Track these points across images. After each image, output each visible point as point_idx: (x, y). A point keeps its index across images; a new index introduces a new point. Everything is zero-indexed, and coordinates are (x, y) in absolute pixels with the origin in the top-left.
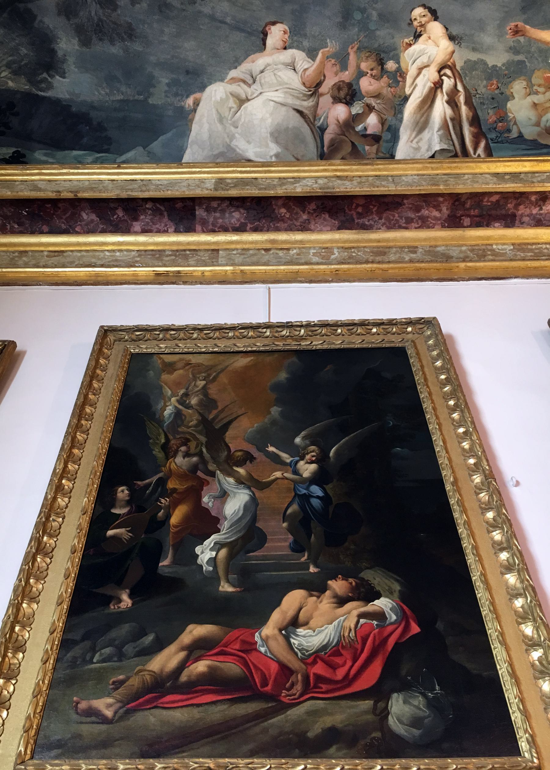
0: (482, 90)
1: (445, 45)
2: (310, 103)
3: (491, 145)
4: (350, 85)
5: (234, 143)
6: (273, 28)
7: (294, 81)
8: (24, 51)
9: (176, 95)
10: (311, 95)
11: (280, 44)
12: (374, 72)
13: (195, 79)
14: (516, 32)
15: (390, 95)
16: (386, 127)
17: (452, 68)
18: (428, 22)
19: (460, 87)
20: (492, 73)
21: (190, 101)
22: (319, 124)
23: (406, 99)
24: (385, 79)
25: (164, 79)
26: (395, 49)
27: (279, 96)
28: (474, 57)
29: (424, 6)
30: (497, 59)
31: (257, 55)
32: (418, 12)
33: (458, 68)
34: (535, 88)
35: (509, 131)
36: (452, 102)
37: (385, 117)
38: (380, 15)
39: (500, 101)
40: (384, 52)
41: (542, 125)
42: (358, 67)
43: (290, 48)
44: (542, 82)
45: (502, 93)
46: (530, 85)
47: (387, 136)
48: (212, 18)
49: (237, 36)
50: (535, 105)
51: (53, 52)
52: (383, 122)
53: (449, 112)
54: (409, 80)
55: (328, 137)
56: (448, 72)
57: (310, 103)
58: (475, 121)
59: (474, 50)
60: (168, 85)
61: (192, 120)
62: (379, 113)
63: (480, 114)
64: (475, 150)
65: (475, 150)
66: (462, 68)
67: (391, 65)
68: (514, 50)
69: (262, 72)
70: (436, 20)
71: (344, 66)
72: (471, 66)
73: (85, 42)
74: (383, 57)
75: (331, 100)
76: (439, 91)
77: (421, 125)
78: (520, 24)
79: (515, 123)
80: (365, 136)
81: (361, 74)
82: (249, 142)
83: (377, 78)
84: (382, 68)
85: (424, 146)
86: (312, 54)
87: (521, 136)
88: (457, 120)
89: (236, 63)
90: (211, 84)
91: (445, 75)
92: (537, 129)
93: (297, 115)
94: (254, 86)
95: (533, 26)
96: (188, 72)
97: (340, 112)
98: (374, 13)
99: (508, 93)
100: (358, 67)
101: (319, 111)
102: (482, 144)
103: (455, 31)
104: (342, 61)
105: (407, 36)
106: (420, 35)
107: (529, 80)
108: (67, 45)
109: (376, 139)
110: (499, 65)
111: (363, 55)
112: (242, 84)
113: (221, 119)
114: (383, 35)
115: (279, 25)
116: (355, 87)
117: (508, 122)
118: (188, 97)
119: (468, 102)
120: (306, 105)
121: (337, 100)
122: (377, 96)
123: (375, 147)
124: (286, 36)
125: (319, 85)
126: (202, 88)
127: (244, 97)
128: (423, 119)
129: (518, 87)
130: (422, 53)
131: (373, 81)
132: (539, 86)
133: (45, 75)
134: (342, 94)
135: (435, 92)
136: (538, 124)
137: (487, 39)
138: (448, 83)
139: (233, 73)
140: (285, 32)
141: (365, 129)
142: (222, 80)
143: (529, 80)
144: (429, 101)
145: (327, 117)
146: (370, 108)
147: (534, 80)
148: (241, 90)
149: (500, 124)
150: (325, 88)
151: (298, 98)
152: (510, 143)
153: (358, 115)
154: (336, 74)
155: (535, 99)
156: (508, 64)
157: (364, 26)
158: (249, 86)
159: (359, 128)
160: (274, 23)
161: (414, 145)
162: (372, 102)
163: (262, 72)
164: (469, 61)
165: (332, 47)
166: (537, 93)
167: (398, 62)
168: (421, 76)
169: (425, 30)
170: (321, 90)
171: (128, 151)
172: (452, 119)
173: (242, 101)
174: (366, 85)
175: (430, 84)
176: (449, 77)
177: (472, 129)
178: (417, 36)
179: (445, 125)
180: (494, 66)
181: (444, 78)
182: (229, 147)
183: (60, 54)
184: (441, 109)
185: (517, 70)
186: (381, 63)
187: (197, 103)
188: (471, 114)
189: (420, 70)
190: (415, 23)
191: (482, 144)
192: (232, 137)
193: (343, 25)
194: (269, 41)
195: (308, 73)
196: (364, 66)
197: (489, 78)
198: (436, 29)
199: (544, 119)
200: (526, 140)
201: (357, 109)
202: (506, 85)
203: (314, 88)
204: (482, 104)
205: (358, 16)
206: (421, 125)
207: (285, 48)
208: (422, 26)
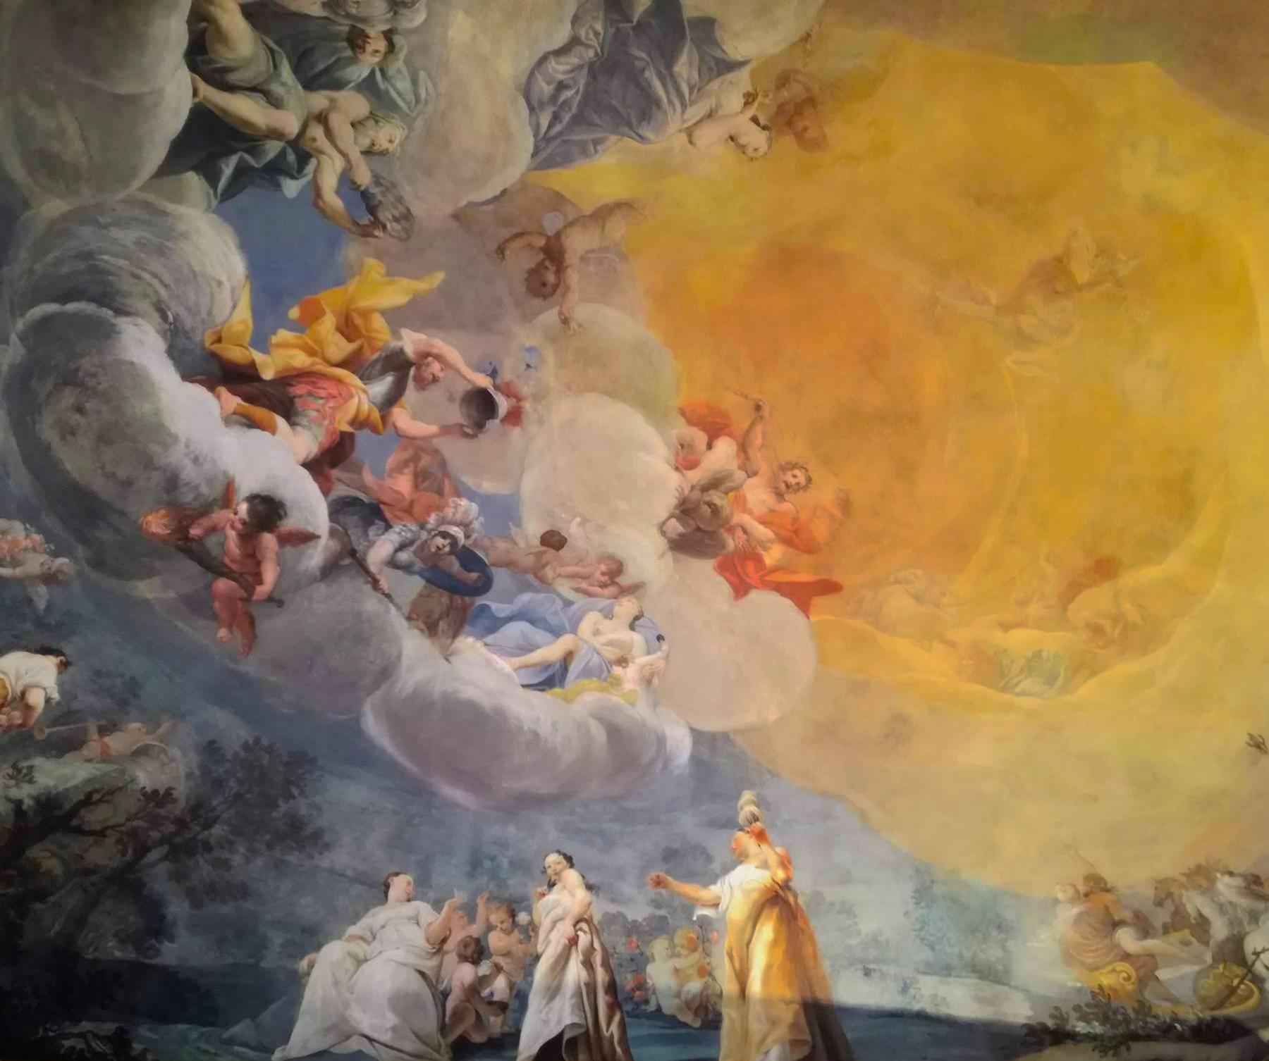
0: (621, 948)
1: (582, 894)
2: (434, 962)
3: (627, 1019)
4: (478, 941)
5: (348, 1013)
6: (396, 879)
7: (418, 937)
8: (132, 919)
9: (290, 956)
10: (435, 954)
11: (405, 896)
12: (505, 926)
13: (310, 937)
14: (659, 883)
15: (521, 954)
16: (515, 992)
17: (589, 921)
18: (562, 870)
19: (597, 945)
20: (632, 929)
21: (304, 964)
22: (441, 987)
23: (537, 958)
24: (516, 932)
25: (277, 939)
26: (528, 900)
27: (400, 955)
28: (613, 909)
29: (559, 852)
30: (638, 912)
31: (378, 909)
32: (553, 858)
33: (596, 921)
34: (678, 949)
35: (647, 1002)
36: (588, 964)
37: (513, 979)
38: (511, 863)
39: (639, 962)
40: (516, 902)
41: (683, 997)
42: (487, 919)
43: (415, 899)
44: (685, 942)
45: (642, 954)
46: (672, 946)
47: (514, 1004)
48: (332, 871)
49: (357, 889)
50: (677, 971)
51: (162, 918)
52: (511, 986)
53: (584, 975)
54: (542, 936)
55: (450, 1004)
56: (584, 926)
57: (434, 962)
58: (612, 988)
59: (613, 900)
60: (282, 946)
61: (305, 985)
62: (508, 975)
63: (617, 979)
64: (609, 1025)
65: (609, 1025)
66: (600, 923)
67: (523, 917)
68: (657, 904)
69: (383, 927)
70: (572, 866)
71: (472, 918)
72: (610, 919)
73: (196, 904)
74: (514, 906)
75: (456, 958)
76: (574, 949)
77: (553, 991)
78: (662, 874)
79: (654, 993)
80: (491, 1003)
81: (490, 928)
82: (364, 1011)
83: (508, 932)
84: (514, 922)
85: (554, 1018)
86: (437, 905)
87: (659, 1009)
88: (591, 987)
89: (355, 918)
90: (327, 942)
91: (581, 929)
92: (677, 1001)
93: (419, 977)
94: (374, 944)
95: (677, 878)
96: (304, 930)
97: (466, 973)
98: (505, 863)
99: (648, 954)
100: (487, 919)
101: (443, 973)
102: (617, 1018)
103: (593, 879)
104: (470, 912)
105: (541, 886)
106: (554, 885)
107: (671, 940)
108: (177, 908)
109: (503, 1007)
110: (640, 920)
111: (493, 906)
112: (361, 943)
113: (336, 983)
114: (515, 884)
115: (402, 876)
116: (483, 943)
117: (647, 990)
118: (302, 958)
119: (606, 964)
120: (429, 965)
121: (463, 958)
122: (507, 954)
123: (501, 1018)
124: (411, 888)
125: (444, 941)
126: (318, 947)
127: (362, 956)
128: (555, 983)
129: (659, 946)
130: (556, 904)
131: (502, 935)
132: (682, 947)
133: (153, 941)
134: (469, 951)
135: (570, 949)
136: (678, 995)
137: (627, 888)
138: (584, 939)
139: (353, 930)
140: (409, 883)
141: (492, 994)
142: (339, 938)
143: (671, 940)
144: (562, 962)
145: (451, 979)
146: (498, 969)
147: (677, 940)
148: (360, 949)
149: (638, 993)
150: (451, 945)
151: (421, 957)
152: (648, 1018)
153: (485, 976)
154: (463, 928)
155: (680, 963)
156: (650, 919)
157: (494, 875)
158: (369, 943)
159: (485, 993)
160: (397, 874)
161: (543, 1016)
162: (502, 961)
163: (383, 927)
164: (607, 913)
165: (460, 897)
166: (679, 956)
167: (530, 913)
168: (555, 931)
169: (560, 880)
170: (446, 947)
171: (236, 1023)
172: (587, 985)
173: (360, 962)
174: (496, 941)
175: (564, 941)
176: (585, 932)
177: (607, 998)
178: (551, 885)
179: (578, 994)
180: (635, 922)
181: (579, 933)
182: (344, 1019)
183: (169, 917)
184: (575, 972)
185: (659, 927)
186: (513, 914)
187: (311, 965)
188: (607, 979)
189: (554, 923)
190: (549, 871)
191: (617, 1018)
192: (346, 1005)
193: (472, 875)
194: (392, 893)
195: (432, 928)
196: (494, 919)
197: (629, 935)
198: (572, 876)
199: (686, 988)
200: (665, 1016)
201: (485, 968)
202: (648, 943)
203: (439, 946)
204: (620, 965)
205: (487, 864)
206: (553, 991)
207: (409, 900)
208: (556, 874)
